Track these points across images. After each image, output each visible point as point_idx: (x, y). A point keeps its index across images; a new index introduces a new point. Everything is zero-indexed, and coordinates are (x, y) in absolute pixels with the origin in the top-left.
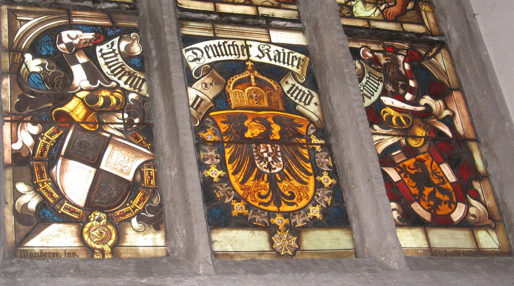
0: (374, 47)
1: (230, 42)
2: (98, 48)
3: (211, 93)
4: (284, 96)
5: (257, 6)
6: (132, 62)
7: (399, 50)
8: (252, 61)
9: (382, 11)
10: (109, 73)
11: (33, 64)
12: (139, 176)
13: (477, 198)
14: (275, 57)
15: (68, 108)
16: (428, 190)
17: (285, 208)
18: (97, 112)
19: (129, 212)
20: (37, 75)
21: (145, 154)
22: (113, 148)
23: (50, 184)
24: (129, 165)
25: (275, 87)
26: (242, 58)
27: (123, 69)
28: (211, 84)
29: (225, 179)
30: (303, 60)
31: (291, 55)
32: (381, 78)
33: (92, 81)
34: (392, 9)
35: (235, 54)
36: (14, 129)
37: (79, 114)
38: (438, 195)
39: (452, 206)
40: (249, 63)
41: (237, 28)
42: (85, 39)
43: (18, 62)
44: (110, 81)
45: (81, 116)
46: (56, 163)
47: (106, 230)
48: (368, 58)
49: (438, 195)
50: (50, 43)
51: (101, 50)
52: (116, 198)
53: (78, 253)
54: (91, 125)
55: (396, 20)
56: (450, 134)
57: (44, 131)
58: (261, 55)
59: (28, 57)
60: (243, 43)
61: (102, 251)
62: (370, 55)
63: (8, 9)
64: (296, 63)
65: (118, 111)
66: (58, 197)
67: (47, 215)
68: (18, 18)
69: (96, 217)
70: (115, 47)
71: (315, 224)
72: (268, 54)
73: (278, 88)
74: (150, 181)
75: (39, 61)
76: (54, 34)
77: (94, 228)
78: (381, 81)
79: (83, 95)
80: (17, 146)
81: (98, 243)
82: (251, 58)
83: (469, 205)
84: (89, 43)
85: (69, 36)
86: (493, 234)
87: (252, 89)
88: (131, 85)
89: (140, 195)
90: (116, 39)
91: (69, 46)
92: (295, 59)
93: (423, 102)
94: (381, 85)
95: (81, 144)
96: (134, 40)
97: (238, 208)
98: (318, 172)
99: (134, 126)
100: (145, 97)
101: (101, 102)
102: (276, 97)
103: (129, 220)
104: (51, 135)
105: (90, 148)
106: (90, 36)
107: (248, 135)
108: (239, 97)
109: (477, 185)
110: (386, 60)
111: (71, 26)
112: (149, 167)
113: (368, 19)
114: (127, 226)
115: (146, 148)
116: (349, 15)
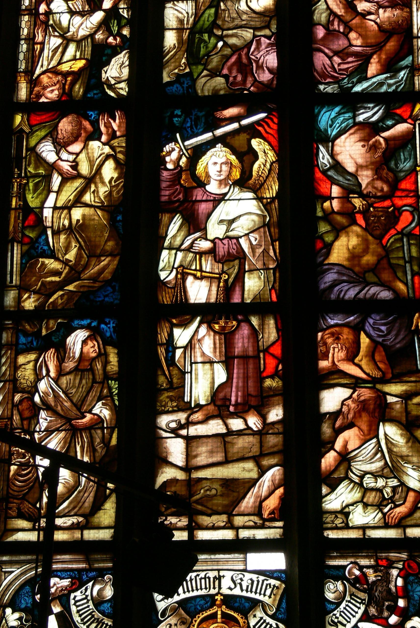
0: (364, 562)
1: (202, 575)
2: (72, 596)
5: (237, 529)
6: (102, 608)
7: (394, 562)
8: (222, 595)
9: (384, 514)
10: (80, 621)
14: (248, 587)
25: (241, 621)
26: (213, 592)
27: (93, 616)
28: (176, 625)
30: (277, 588)
31: (266, 582)
32: (365, 600)
34: (398, 510)
35: (206, 588)
40: (219, 598)
41: (213, 557)
42: (61, 587)
48: (353, 577)
50: (30, 594)
51: (75, 597)
55: (401, 524)
58: (233, 586)
59: (9, 611)
60: (216, 573)
62: (357, 573)
64: (268, 592)
68: (3, 570)
70: (88, 593)
72: (241, 584)
73: (244, 622)
75: (17, 615)
78: (363, 604)
82: (221, 591)
84: (64, 590)
87: (218, 626)
90: (90, 584)
92: (268, 587)
94: (363, 607)
106: (66, 582)
110: (375, 576)
113: (364, 528)
116: (343, 525)
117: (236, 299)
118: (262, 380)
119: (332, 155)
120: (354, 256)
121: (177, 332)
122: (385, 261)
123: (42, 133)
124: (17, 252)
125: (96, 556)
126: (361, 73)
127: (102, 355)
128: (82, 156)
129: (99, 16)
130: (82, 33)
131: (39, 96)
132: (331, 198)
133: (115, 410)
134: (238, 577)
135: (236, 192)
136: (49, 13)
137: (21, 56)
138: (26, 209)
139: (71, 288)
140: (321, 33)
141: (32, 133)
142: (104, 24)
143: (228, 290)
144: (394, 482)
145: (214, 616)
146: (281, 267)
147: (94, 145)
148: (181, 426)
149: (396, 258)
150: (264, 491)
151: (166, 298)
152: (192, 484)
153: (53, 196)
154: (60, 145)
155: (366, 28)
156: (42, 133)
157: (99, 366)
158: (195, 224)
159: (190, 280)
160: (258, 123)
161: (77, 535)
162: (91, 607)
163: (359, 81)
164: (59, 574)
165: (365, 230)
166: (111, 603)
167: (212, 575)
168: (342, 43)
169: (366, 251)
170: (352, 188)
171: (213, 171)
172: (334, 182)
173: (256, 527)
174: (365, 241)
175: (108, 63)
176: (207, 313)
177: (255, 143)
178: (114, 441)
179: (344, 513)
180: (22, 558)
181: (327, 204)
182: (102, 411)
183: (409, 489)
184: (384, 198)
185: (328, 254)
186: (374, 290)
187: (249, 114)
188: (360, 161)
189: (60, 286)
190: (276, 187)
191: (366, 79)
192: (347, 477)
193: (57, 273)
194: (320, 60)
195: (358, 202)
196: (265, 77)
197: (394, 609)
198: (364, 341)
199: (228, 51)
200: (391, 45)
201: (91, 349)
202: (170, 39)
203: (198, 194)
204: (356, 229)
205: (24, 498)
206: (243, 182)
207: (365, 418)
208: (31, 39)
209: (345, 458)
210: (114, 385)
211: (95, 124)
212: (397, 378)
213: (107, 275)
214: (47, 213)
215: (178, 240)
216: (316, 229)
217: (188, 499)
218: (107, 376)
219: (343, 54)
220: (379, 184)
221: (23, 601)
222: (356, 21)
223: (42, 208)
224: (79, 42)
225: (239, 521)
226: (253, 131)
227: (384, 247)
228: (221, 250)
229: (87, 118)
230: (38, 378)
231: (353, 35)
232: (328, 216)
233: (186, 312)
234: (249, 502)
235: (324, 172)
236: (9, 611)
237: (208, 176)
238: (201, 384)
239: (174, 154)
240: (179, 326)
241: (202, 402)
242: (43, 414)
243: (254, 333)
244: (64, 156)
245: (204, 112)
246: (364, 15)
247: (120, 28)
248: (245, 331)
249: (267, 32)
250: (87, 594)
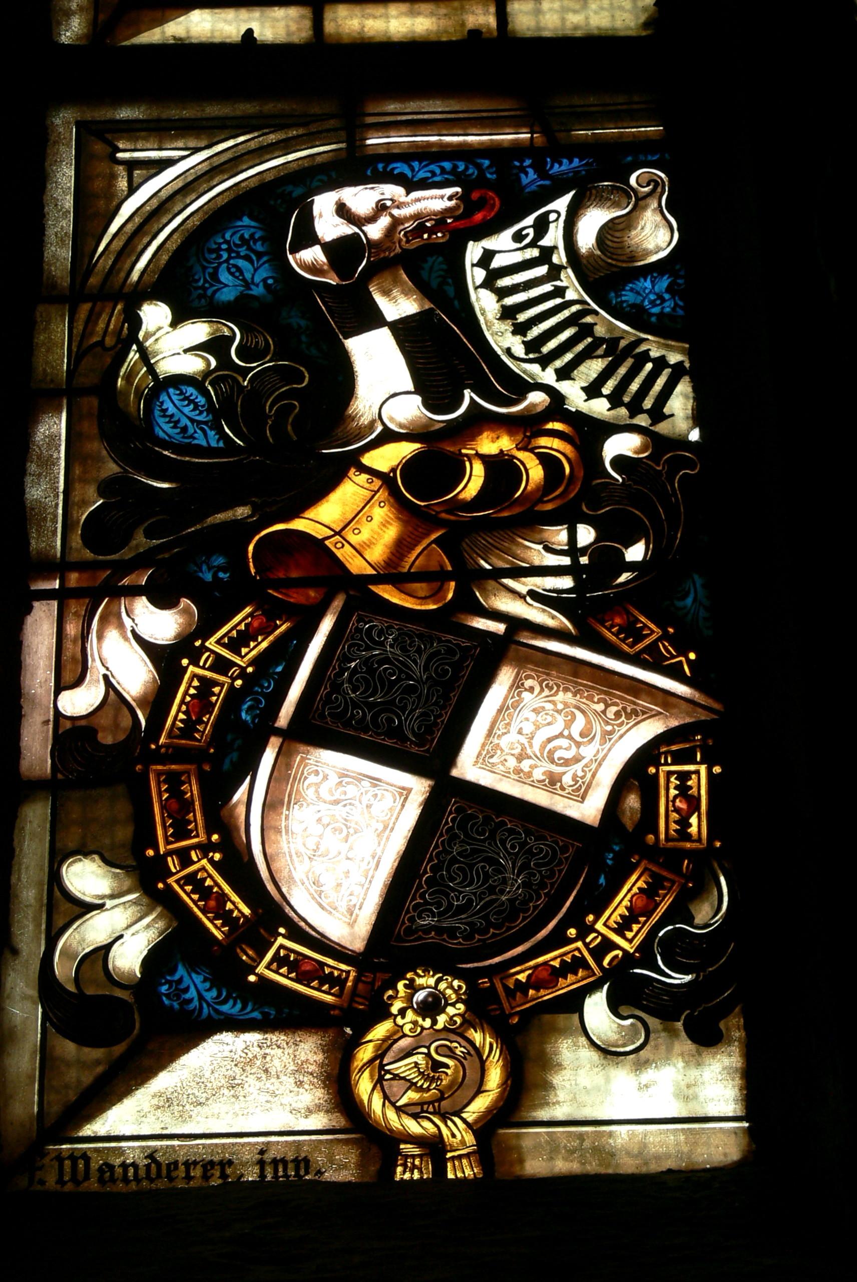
2: (474, 251)
6: (628, 297)
10: (519, 350)
11: (174, 344)
12: (633, 801)
15: (324, 516)
18: (456, 527)
19: (578, 963)
20: (190, 390)
21: (665, 698)
22: (517, 685)
23: (217, 856)
24: (588, 751)
27: (586, 330)
36: (72, 629)
37: (369, 544)
42: (416, 216)
43: (109, 341)
44: (522, 387)
45: (377, 554)
46: (248, 766)
47: (459, 1051)
50: (259, 247)
51: (488, 255)
52: (514, 909)
53: (320, 1159)
54: (421, 588)
57: (205, 628)
59: (155, 315)
61: (435, 1148)
63: (78, 124)
65: (554, 519)
66: (247, 911)
67: (192, 993)
68: (120, 155)
69: (420, 996)
70: (554, 236)
74: (684, 823)
75: (199, 331)
76: (279, 208)
77: (404, 1043)
79: (387, 458)
80: (79, 702)
81: (416, 1112)
84: (432, 231)
85: (342, 210)
88: (615, 400)
89: (634, 884)
90: (561, 204)
91: (343, 252)
95: (371, 671)
96: (640, 202)
99: (624, 577)
100: (682, 443)
101: (474, 482)
103: (573, 1003)
104: (235, 645)
105: (411, 690)
106: (436, 201)
112: (681, 757)
114: (564, 1032)
115: (674, 673)
125: (576, 101)
162: (570, 295)
164: (400, 168)
166: (674, 274)
180: (213, 110)
221: (225, 276)
236: (155, 315)
250: (546, 242)
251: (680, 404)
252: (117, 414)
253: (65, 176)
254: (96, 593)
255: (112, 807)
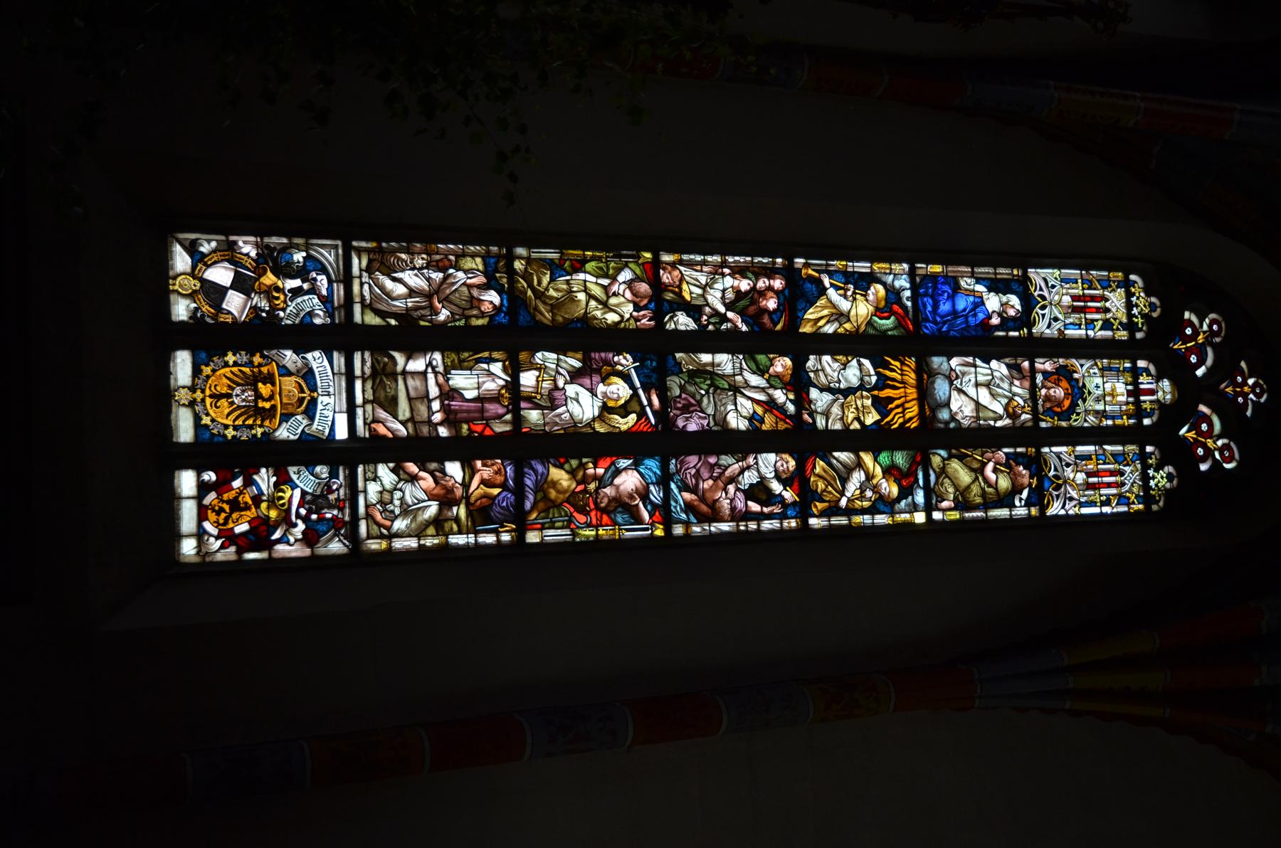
0: (342, 491)
3: (290, 366)
4: (293, 415)
11: (299, 257)
13: (223, 547)
15: (269, 274)
16: (226, 507)
17: (208, 401)
18: (269, 292)
29: (226, 365)
33: (289, 291)
38: (223, 515)
39: (217, 524)
49: (223, 515)
56: (274, 537)
59: (304, 254)
62: (335, 487)
71: (197, 418)
76: (323, 270)
79: (280, 284)
80: (241, 244)
83: (217, 538)
86: (193, 552)
91: (315, 279)
93: (299, 522)
97: (207, 370)
98: (236, 428)
101: (275, 294)
102: (291, 409)
106: (324, 292)
107: (260, 385)
108: (289, 384)
109: (233, 549)
111: (330, 282)
113: (365, 491)
117: (523, 405)
118: (467, 422)
119: (625, 469)
120: (554, 484)
121: (500, 365)
122: (550, 504)
123: (638, 272)
124: (552, 255)
126: (684, 487)
127: (483, 315)
128: (622, 299)
129: (722, 309)
130: (709, 298)
131: (664, 269)
132: (595, 467)
133: (444, 324)
134: (330, 407)
135: (598, 404)
136: (723, 275)
137: (692, 257)
138: (584, 261)
139: (529, 293)
140: (712, 460)
141: (638, 265)
142: (716, 313)
143: (529, 399)
144: (397, 511)
145: (302, 391)
146: (546, 435)
147: (631, 307)
148: (433, 368)
149: (554, 512)
150: (389, 424)
151: (523, 356)
152: (393, 376)
153: (594, 279)
154: (629, 284)
155: (716, 491)
156: (638, 272)
157: (475, 312)
158: (575, 376)
159: (537, 373)
160: (648, 418)
161: (357, 299)
163: (678, 487)
165: (573, 491)
167: (331, 390)
168: (705, 474)
169: (558, 492)
170: (601, 482)
171: (613, 388)
172: (607, 470)
173: (365, 419)
174: (565, 491)
175: (688, 316)
176: (513, 385)
177: (633, 417)
178: (422, 323)
179: (375, 478)
180: (341, 263)
181: (591, 465)
182: (444, 315)
183: (393, 521)
184: (596, 504)
185: (555, 466)
186: (531, 497)
187: (654, 412)
188: (622, 488)
189: (531, 286)
190: (602, 430)
191: (680, 492)
192: (400, 480)
193: (539, 283)
194: (693, 460)
195: (592, 486)
196: (680, 423)
197: (310, 512)
198: (496, 491)
199: (698, 397)
200: (704, 508)
201: (486, 307)
202: (706, 358)
203: (596, 378)
204: (574, 485)
205: (382, 263)
206: (605, 409)
207: (442, 492)
208: (704, 263)
209: (413, 479)
210: (462, 323)
211: (645, 307)
212: (470, 513)
213: (539, 317)
214: (582, 276)
215: (564, 365)
216: (573, 458)
217: (382, 375)
218: (468, 318)
219: (697, 475)
220: (606, 500)
222: (721, 484)
223: (585, 272)
224: (703, 296)
225: (369, 407)
226: (642, 414)
227: (561, 504)
228: (557, 394)
229: (649, 302)
230: (466, 272)
231: (711, 482)
232: (583, 466)
233: (514, 370)
234: (382, 414)
235: (613, 463)
237: (610, 384)
238: (464, 381)
239: (625, 361)
240: (504, 366)
241: (451, 382)
242: (441, 275)
243: (500, 417)
244: (623, 287)
245: (655, 379)
246: (725, 489)
247: (714, 324)
248: (501, 411)
249: (712, 424)
251: (289, 322)
252: (285, 249)
253: (328, 242)
254: (257, 245)
255: (225, 247)
